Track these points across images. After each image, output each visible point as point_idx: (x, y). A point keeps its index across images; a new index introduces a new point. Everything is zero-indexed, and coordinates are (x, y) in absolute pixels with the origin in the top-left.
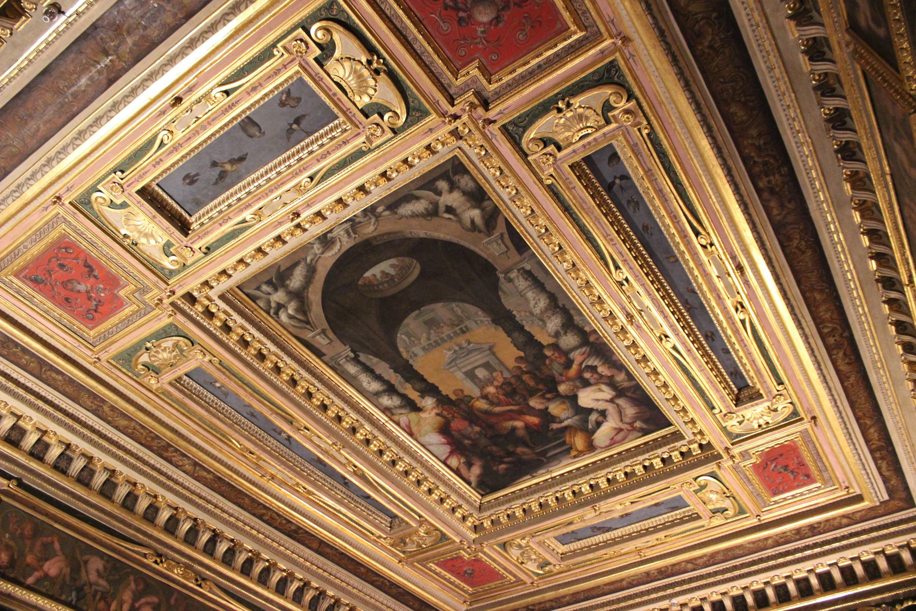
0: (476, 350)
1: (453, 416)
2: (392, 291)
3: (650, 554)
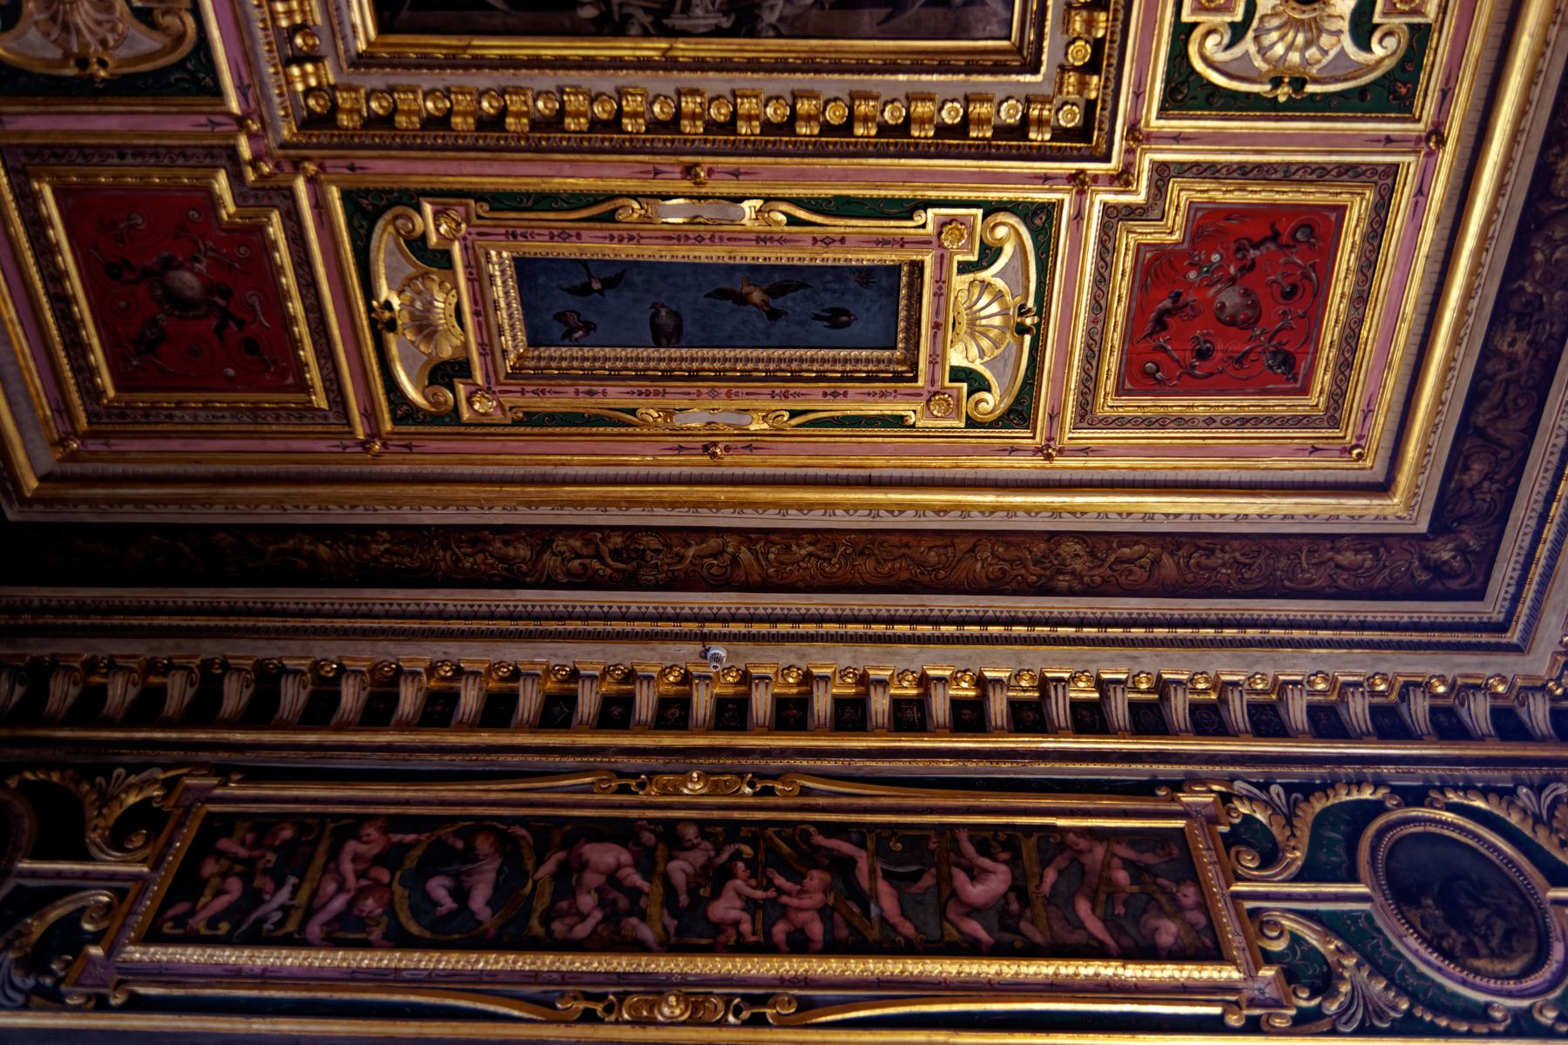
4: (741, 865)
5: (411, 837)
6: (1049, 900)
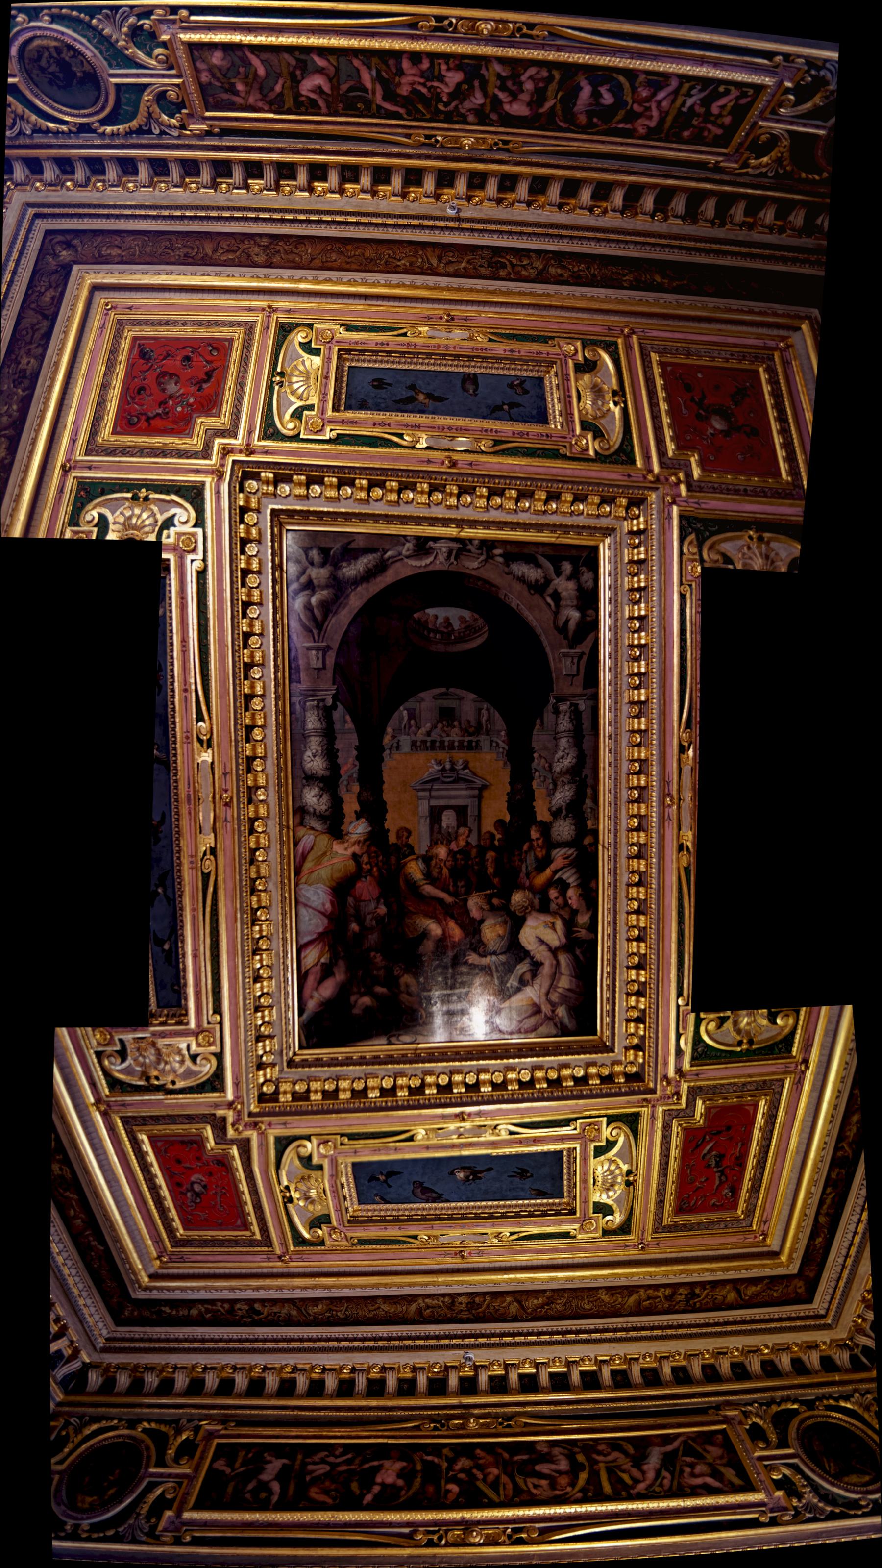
0: (466, 781)
1: (370, 871)
2: (440, 648)
4: (445, 99)
5: (621, 126)
6: (279, 75)
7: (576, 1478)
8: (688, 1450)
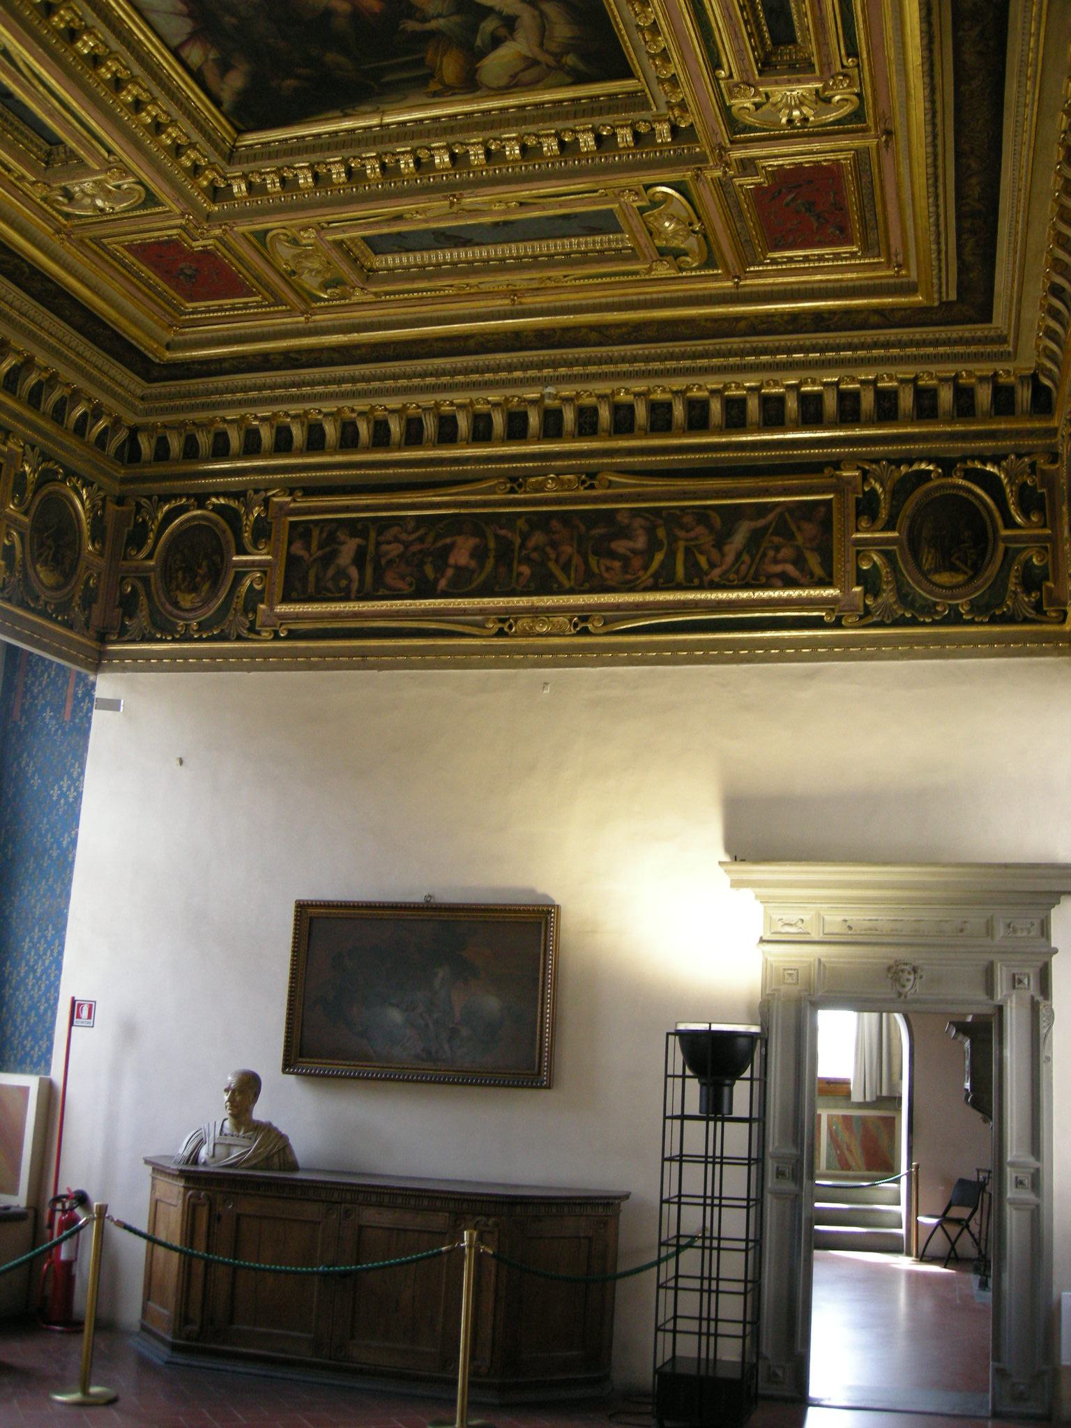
3: (530, 301)
7: (652, 559)
8: (782, 529)
